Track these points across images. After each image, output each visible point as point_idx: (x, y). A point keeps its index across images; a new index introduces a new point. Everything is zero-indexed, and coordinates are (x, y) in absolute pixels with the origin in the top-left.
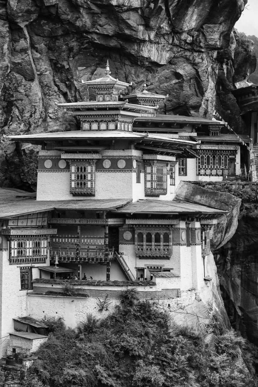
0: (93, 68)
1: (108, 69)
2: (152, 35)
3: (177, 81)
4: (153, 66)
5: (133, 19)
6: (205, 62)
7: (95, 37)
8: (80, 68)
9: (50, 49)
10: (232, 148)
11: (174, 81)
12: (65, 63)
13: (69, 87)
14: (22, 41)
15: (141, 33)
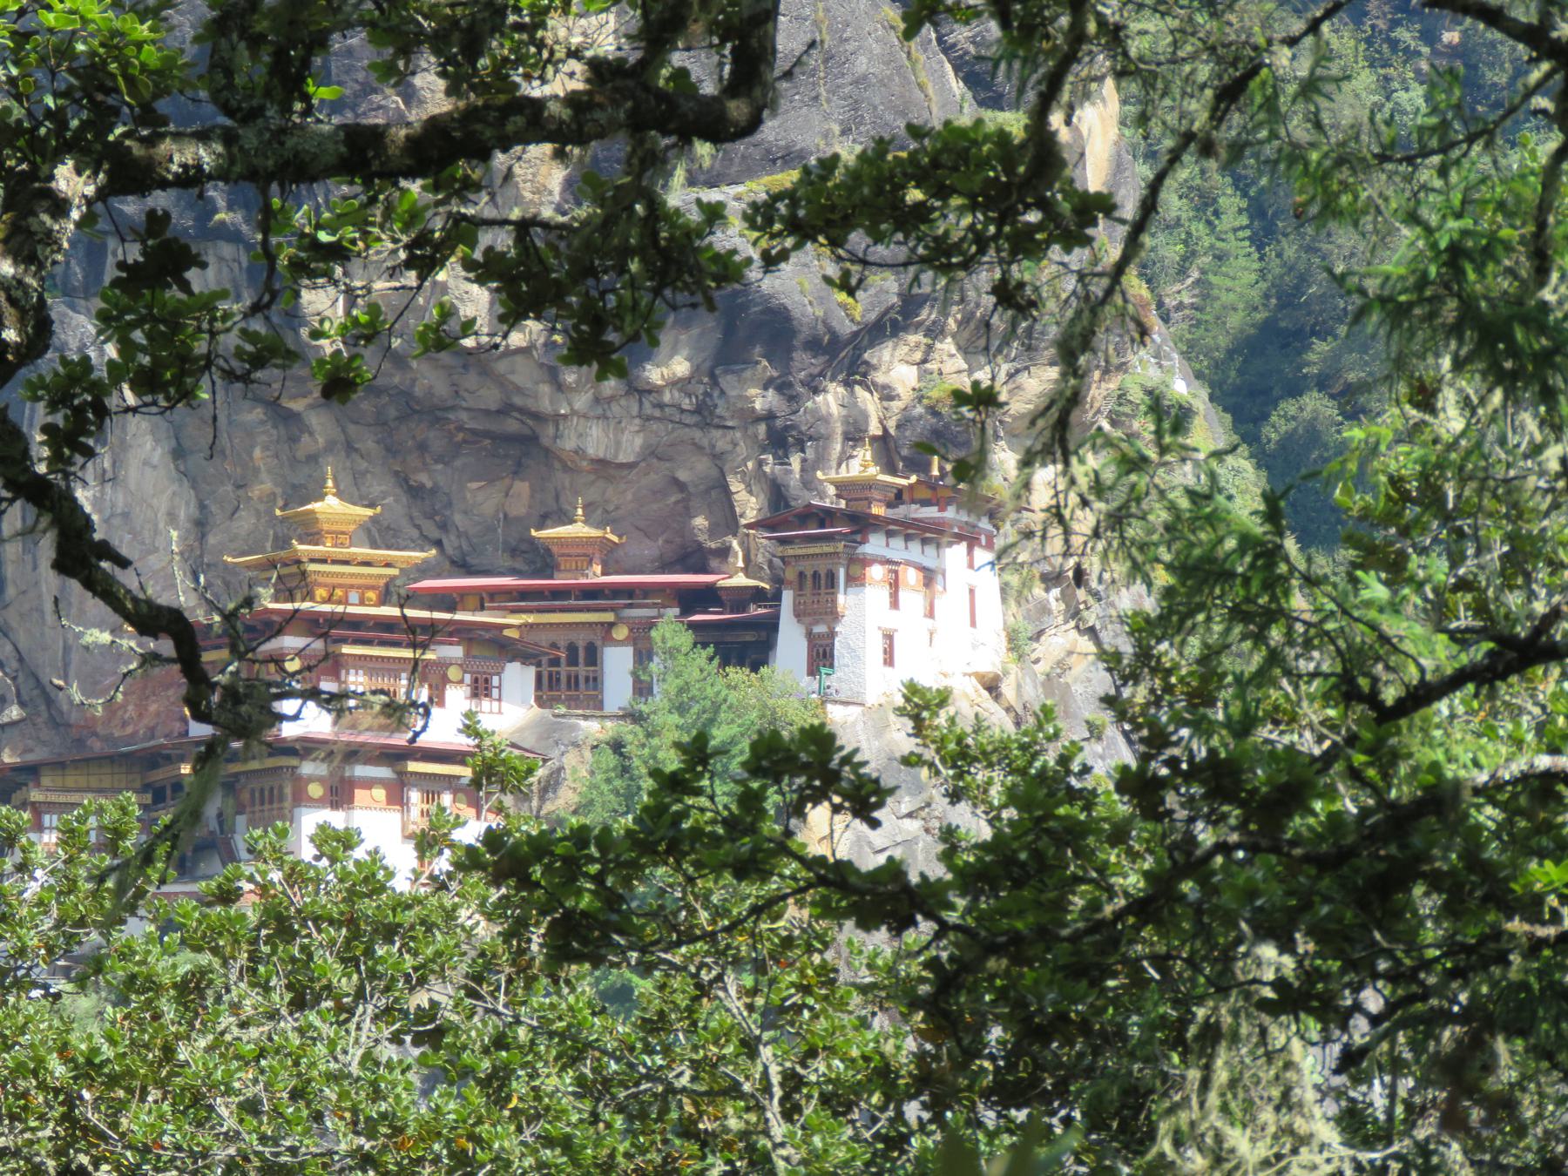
0: (507, 481)
1: (330, 483)
2: (582, 401)
3: (679, 496)
4: (604, 467)
5: (523, 374)
6: (742, 449)
7: (464, 416)
8: (474, 485)
9: (388, 450)
10: (749, 637)
11: (673, 499)
12: (424, 478)
13: (443, 527)
14: (305, 438)
15: (545, 399)
